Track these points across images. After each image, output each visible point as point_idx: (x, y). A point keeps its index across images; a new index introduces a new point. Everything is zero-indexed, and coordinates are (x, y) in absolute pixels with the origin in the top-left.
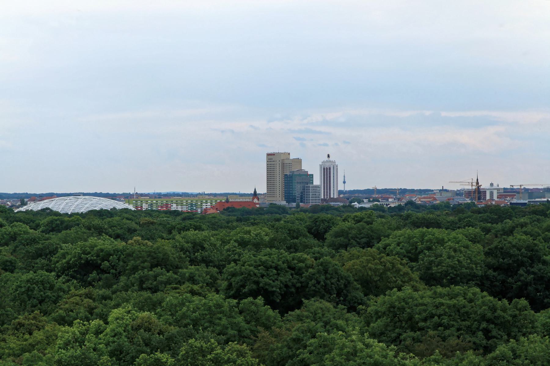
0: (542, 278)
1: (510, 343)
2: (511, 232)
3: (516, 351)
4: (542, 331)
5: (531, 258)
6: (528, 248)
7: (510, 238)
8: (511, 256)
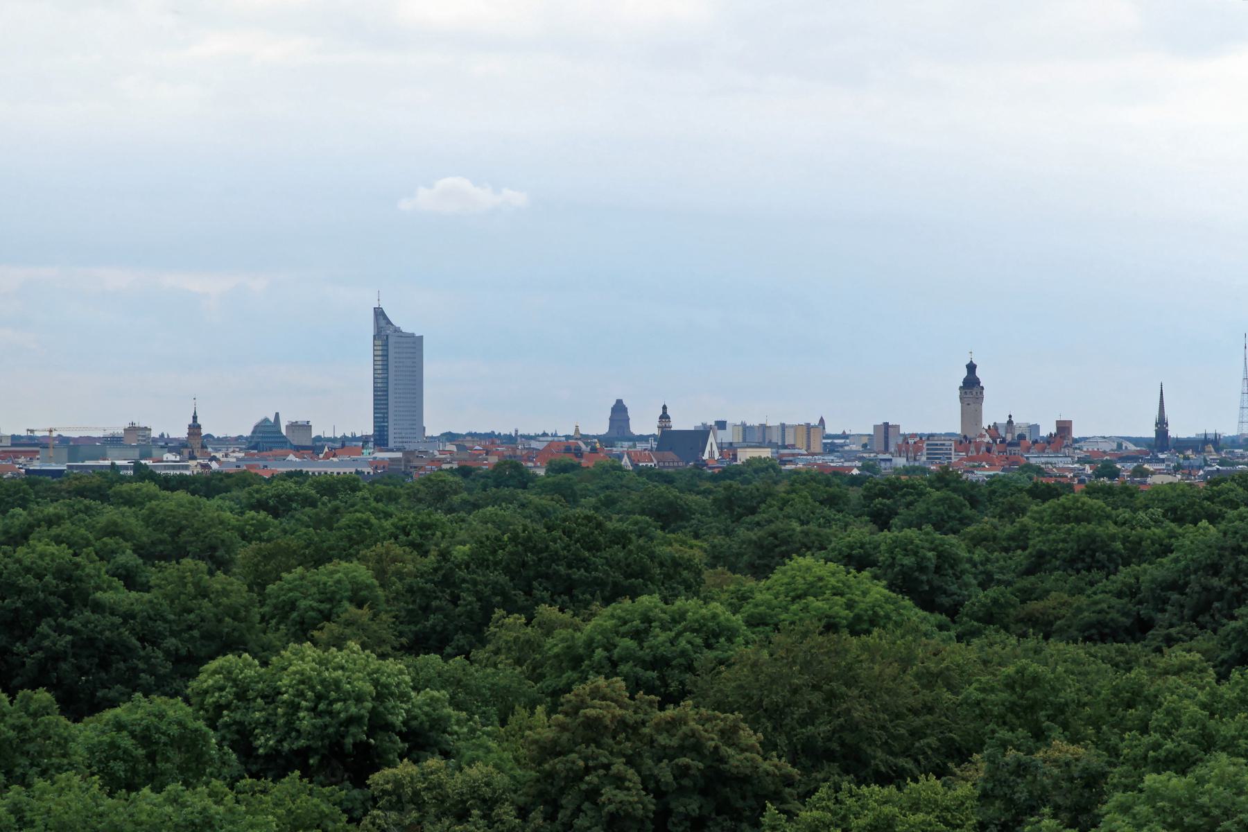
0: (91, 642)
1: (11, 793)
2: (22, 537)
3: (23, 811)
4: (87, 762)
5: (66, 596)
6: (60, 574)
7: (21, 551)
8: (20, 591)
